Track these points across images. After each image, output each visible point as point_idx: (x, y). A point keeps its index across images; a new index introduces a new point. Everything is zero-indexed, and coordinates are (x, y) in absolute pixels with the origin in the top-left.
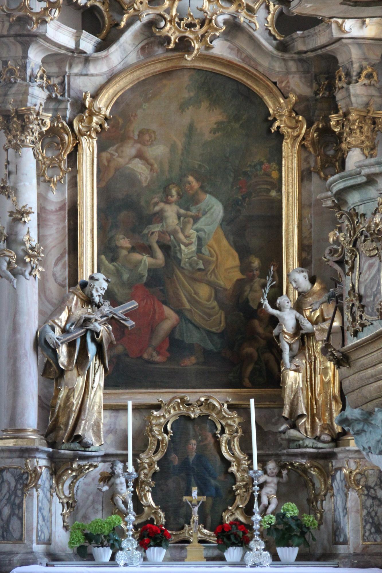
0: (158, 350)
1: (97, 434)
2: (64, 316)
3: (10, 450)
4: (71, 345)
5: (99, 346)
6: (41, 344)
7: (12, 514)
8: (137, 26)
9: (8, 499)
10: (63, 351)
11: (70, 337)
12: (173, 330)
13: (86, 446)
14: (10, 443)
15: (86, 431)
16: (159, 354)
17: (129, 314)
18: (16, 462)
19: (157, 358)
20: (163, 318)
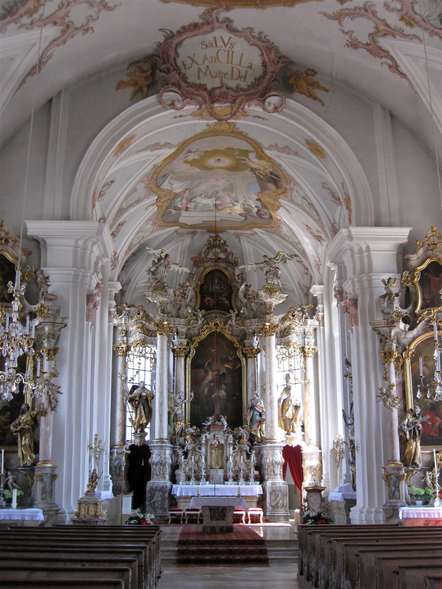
0: (435, 432)
1: (420, 462)
2: (407, 420)
3: (393, 468)
4: (410, 432)
5: (419, 431)
6: (400, 430)
7: (396, 489)
8: (423, 322)
9: (394, 485)
10: (408, 433)
11: (410, 428)
12: (440, 425)
13: (417, 466)
14: (393, 465)
15: (417, 461)
16: (436, 433)
17: (427, 419)
18: (396, 471)
19: (435, 435)
20: (437, 421)
